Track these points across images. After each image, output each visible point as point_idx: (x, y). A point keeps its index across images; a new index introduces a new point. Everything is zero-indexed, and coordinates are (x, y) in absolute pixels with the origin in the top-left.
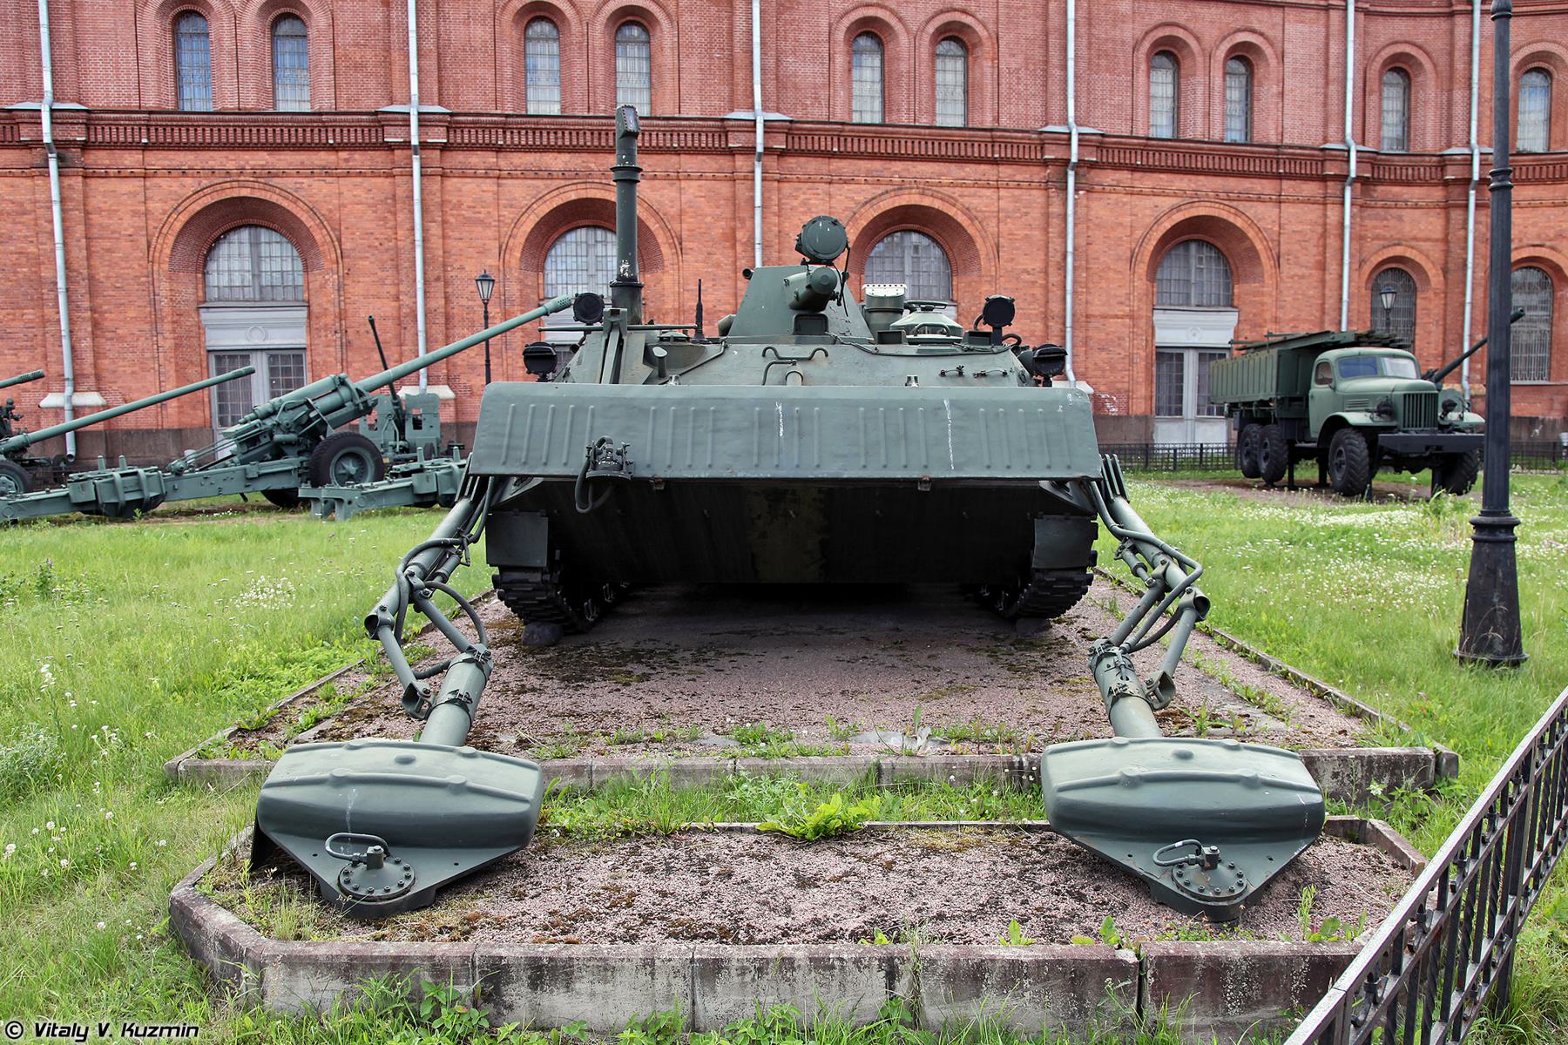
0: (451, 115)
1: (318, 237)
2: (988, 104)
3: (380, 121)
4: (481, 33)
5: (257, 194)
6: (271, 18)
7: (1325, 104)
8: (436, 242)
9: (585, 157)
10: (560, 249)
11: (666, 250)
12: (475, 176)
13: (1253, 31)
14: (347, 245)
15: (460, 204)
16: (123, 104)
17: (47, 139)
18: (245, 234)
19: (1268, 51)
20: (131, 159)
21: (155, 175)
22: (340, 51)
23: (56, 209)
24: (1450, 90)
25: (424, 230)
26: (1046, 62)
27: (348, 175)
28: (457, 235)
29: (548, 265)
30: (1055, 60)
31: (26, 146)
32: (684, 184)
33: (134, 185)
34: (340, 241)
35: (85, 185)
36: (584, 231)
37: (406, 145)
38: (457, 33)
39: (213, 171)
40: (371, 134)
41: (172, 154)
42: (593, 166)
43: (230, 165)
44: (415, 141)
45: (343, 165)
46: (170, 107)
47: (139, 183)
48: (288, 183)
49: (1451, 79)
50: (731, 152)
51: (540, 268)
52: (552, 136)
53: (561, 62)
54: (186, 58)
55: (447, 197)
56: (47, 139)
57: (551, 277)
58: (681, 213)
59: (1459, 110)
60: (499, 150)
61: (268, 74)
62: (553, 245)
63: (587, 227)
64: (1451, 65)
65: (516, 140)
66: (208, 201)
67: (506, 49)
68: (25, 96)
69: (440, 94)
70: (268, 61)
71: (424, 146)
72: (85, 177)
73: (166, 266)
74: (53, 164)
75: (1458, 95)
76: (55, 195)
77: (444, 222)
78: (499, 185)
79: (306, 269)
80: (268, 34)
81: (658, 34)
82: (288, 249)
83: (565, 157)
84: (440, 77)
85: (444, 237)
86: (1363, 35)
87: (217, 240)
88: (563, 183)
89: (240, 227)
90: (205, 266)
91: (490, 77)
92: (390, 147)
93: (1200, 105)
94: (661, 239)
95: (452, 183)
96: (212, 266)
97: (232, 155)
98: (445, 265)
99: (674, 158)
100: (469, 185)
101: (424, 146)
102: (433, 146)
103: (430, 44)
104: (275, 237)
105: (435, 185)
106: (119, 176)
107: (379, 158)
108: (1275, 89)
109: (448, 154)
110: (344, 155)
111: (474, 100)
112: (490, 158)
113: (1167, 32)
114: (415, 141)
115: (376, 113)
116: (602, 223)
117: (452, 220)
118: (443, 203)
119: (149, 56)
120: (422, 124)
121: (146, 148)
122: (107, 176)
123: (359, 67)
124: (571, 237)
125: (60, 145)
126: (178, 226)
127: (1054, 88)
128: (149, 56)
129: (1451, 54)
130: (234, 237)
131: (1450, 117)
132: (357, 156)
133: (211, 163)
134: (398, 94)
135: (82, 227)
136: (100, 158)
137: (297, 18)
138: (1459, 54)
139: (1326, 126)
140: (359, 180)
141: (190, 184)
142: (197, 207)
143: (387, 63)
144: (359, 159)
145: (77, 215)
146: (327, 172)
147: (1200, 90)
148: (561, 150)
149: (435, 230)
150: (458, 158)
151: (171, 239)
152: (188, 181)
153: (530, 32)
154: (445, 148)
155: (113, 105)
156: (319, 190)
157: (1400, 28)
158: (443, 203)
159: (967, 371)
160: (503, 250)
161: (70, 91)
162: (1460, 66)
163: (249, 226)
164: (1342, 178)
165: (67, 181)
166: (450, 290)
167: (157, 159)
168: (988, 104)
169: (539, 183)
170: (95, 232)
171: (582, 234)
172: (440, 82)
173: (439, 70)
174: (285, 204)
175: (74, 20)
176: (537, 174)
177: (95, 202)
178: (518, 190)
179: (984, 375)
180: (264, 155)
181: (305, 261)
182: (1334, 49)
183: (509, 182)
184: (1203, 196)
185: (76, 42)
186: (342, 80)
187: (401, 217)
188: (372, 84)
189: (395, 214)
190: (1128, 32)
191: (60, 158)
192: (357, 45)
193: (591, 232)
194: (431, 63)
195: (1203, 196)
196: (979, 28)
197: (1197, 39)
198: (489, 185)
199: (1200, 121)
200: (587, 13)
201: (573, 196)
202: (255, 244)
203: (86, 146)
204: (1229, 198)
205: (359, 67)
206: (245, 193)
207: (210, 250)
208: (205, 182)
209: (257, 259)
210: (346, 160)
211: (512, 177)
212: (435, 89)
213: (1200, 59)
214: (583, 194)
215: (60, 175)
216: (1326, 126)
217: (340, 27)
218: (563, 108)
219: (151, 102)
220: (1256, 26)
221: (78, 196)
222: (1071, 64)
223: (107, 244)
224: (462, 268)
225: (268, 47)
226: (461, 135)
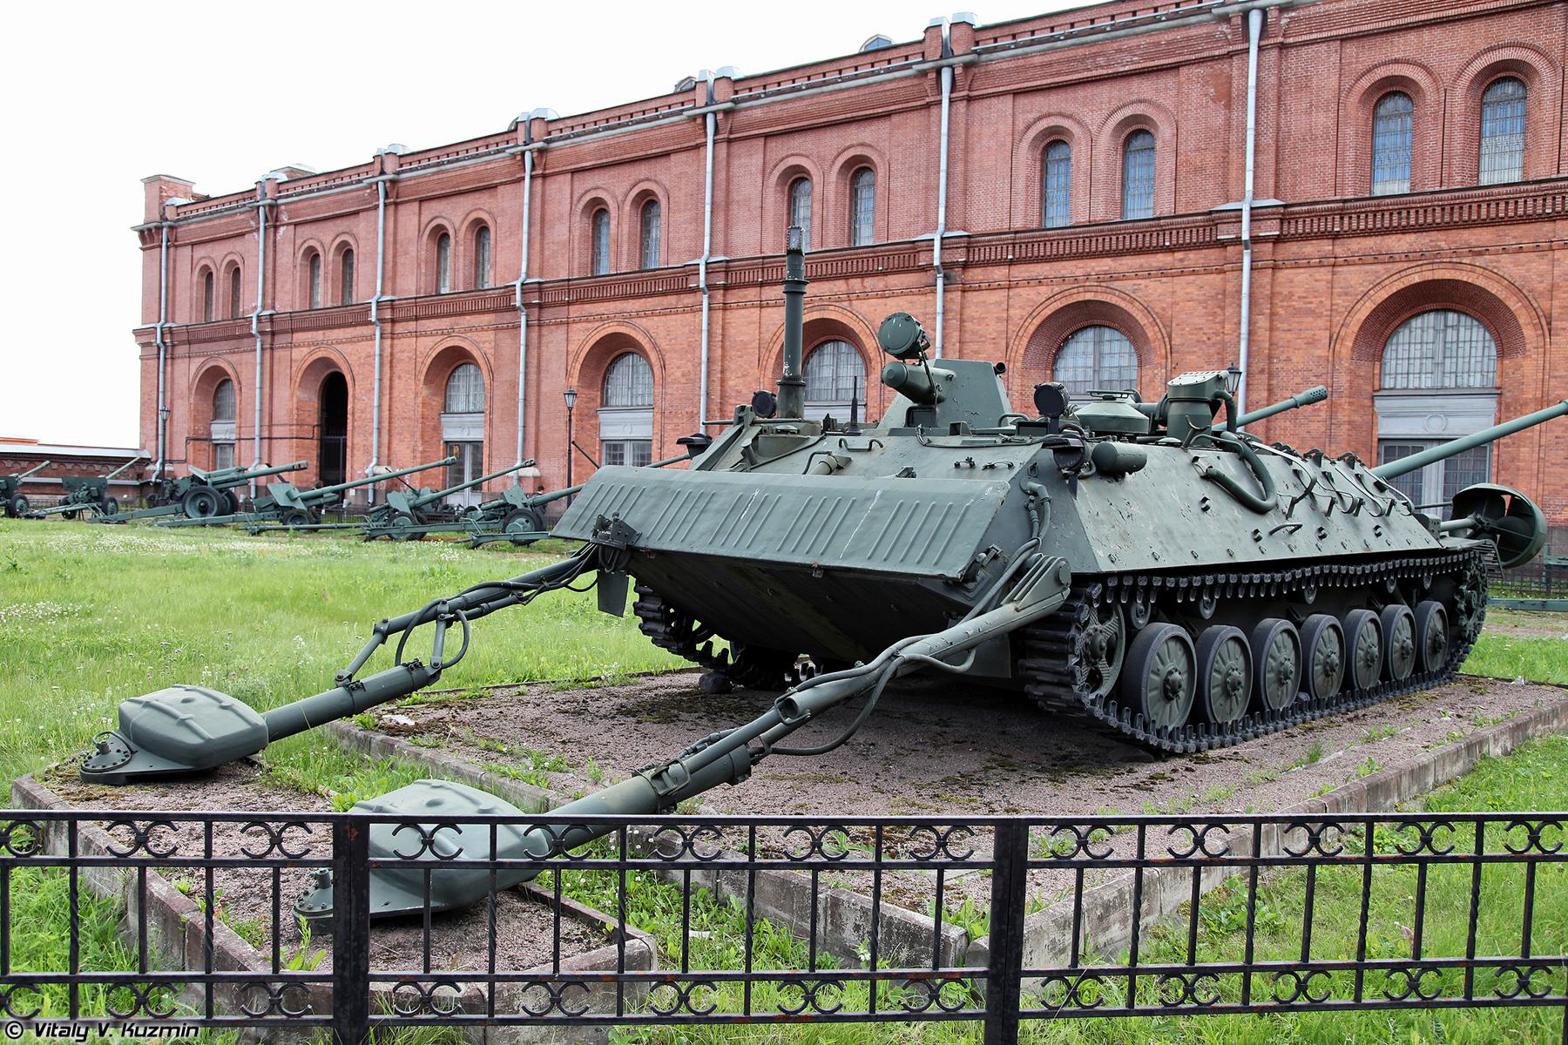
0: (1285, 206)
1: (1150, 334)
3: (1213, 219)
4: (1323, 120)
5: (1100, 298)
6: (1123, 136)
8: (1263, 335)
9: (1434, 235)
10: (1403, 335)
11: (1529, 332)
12: (1309, 266)
14: (1176, 341)
15: (1291, 294)
16: (997, 227)
17: (936, 263)
18: (1090, 334)
20: (999, 273)
21: (1017, 286)
22: (1182, 158)
23: (939, 319)
25: (1251, 322)
28: (1285, 326)
29: (1389, 353)
31: (923, 269)
32: (1558, 254)
33: (1000, 295)
34: (1170, 337)
35: (963, 297)
36: (1432, 316)
37: (1237, 241)
38: (1297, 123)
39: (1063, 278)
40: (1204, 234)
41: (1032, 267)
42: (1443, 244)
43: (1079, 272)
44: (1245, 236)
45: (1178, 265)
46: (1035, 226)
47: (1004, 293)
48: (1127, 285)
50: (1223, 244)
51: (1379, 357)
52: (1395, 217)
53: (1414, 136)
54: (1052, 182)
55: (1278, 289)
56: (936, 263)
57: (1390, 366)
58: (1553, 287)
60: (1335, 237)
61: (1118, 187)
62: (1395, 331)
63: (1437, 311)
65: (1354, 225)
66: (1058, 305)
67: (1349, 132)
68: (926, 230)
69: (1277, 186)
70: (1118, 175)
72: (964, 291)
73: (1019, 365)
74: (940, 282)
76: (939, 309)
77: (1272, 314)
78: (1334, 273)
79: (1140, 365)
80: (1120, 151)
81: (1537, 85)
82: (1126, 346)
83: (1411, 238)
84: (1277, 170)
85: (1271, 329)
87: (1066, 340)
88: (1406, 265)
89: (1086, 328)
90: (1055, 361)
91: (1330, 163)
92: (1223, 244)
94: (1523, 319)
95: (1283, 275)
96: (1061, 364)
97: (1080, 263)
98: (1270, 357)
99: (1548, 226)
100: (1301, 276)
101: (1255, 240)
102: (1265, 239)
103: (1268, 140)
104: (1117, 335)
105: (1265, 278)
106: (989, 289)
107: (1212, 255)
109: (1281, 246)
110: (1179, 255)
111: (1312, 187)
112: (1326, 246)
114: (1245, 236)
115: (1210, 213)
116: (1454, 306)
117: (1281, 311)
118: (1272, 295)
119: (1020, 184)
121: (1011, 263)
122: (980, 289)
123: (1198, 170)
124: (1416, 323)
125: (945, 265)
126: (1032, 329)
128: (1020, 184)
130: (1082, 337)
132: (1192, 255)
133: (1063, 272)
134: (1233, 192)
135: (957, 333)
136: (976, 274)
137: (1147, 132)
142: (1048, 312)
143: (1225, 163)
144: (1194, 258)
145: (955, 323)
146: (1163, 273)
148: (1405, 230)
149: (1262, 322)
150: (1292, 249)
151: (1025, 340)
152: (1043, 289)
153: (1382, 111)
154: (1277, 240)
155: (990, 229)
156: (1154, 290)
158: (1272, 295)
159: (980, 464)
160: (1333, 340)
161: (958, 222)
163: (1094, 326)
164: (696, 290)
165: (949, 296)
166: (1274, 382)
167: (1020, 272)
169: (1379, 267)
170: (967, 337)
171: (1430, 319)
172: (1277, 175)
173: (1277, 163)
174: (1123, 304)
175: (966, 162)
176: (1376, 259)
177: (969, 312)
178: (1355, 277)
179: (992, 467)
180: (1108, 261)
181: (1140, 357)
183: (1345, 269)
184: (1079, 279)
185: (966, 180)
186: (1181, 185)
187: (1229, 311)
188: (1210, 185)
189: (1223, 308)
191: (946, 277)
192: (1198, 150)
193: (1441, 317)
194: (1269, 158)
195: (1079, 279)
198: (1323, 274)
200: (1447, 79)
201: (1417, 279)
202: (1098, 342)
203: (966, 266)
204: (835, 299)
205: (1198, 170)
206: (1089, 296)
207: (1060, 349)
208: (1057, 289)
209: (1098, 356)
210: (1181, 260)
211: (1347, 263)
212: (1272, 182)
214: (1429, 276)
215: (945, 291)
217: (1182, 136)
218: (1413, 185)
219: (1018, 224)
221: (956, 307)
223: (975, 347)
224: (1288, 360)
225: (1119, 163)
226: (1292, 225)
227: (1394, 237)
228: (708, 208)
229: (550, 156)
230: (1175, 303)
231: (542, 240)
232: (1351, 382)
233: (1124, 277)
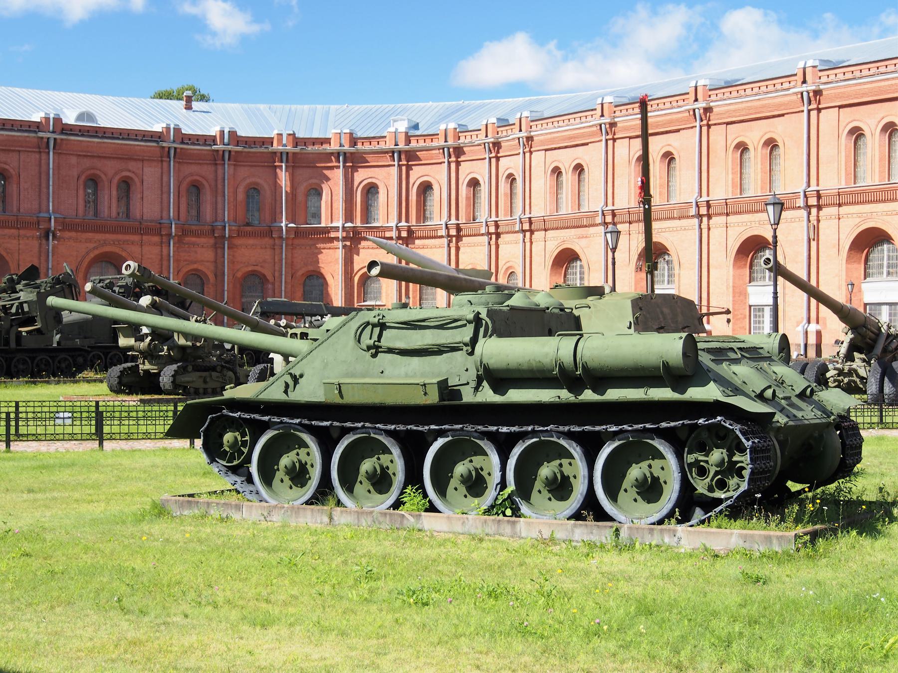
2: (15, 203)
7: (161, 203)
13: (130, 171)
19: (136, 179)
24: (216, 197)
26: (40, 185)
30: (44, 185)
49: (216, 191)
59: (220, 206)
64: (216, 186)
75: (219, 199)
86: (178, 172)
93: (106, 203)
108: (139, 196)
113: (92, 171)
127: (44, 197)
129: (216, 181)
131: (216, 209)
138: (219, 182)
139: (162, 212)
147: (106, 197)
157: (194, 169)
162: (220, 186)
168: (15, 203)
182: (165, 179)
190: (75, 173)
196: (11, 170)
197: (105, 175)
199: (106, 211)
213: (106, 183)
216: (162, 212)
220: (131, 168)
222: (51, 188)
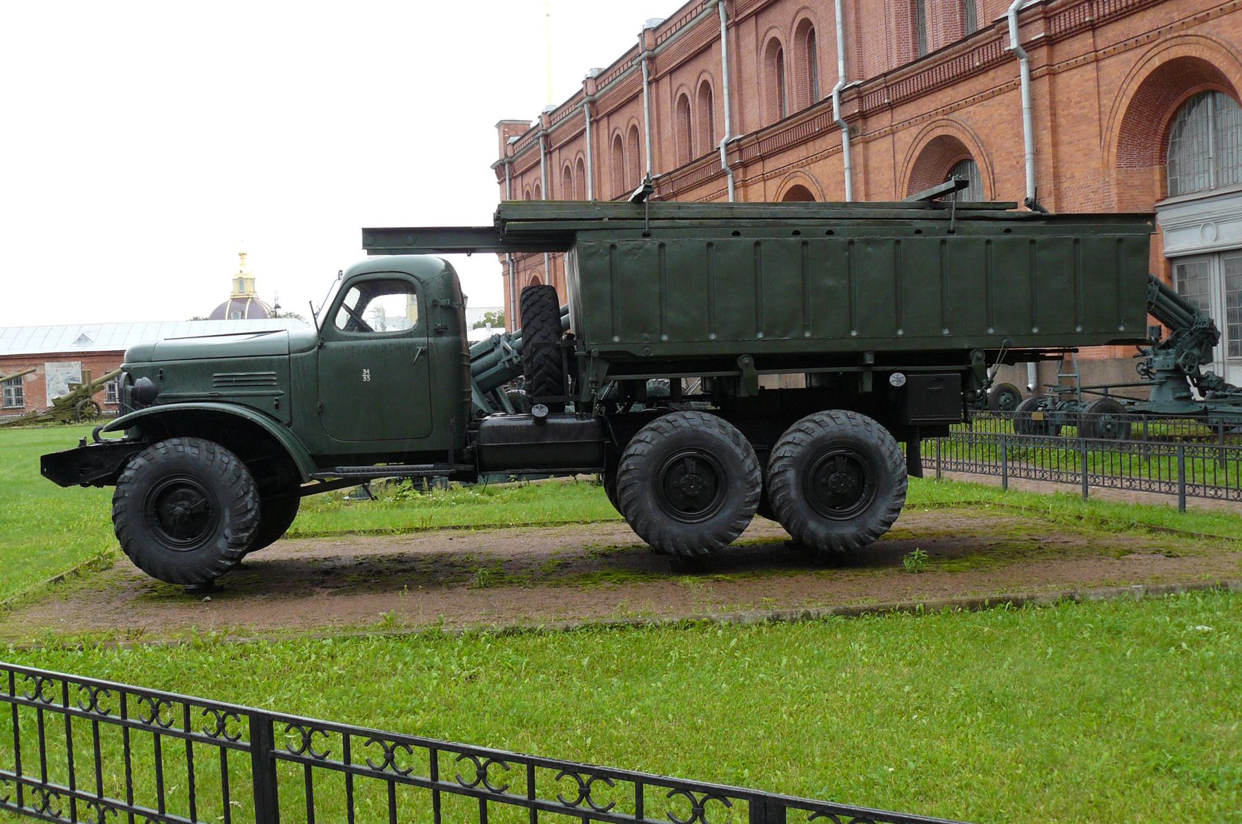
23: (847, 174)
27: (993, 95)
35: (866, 149)
47: (889, 138)
60: (1093, 27)
66: (922, 145)
71: (1029, 47)
105: (1044, 86)
110: (991, 74)
120: (1022, 25)
121: (891, 106)
140: (1002, 97)
141: (914, 130)
142: (917, 154)
145: (861, 176)
150: (1068, 49)
151: (906, 185)
154: (1051, 41)
177: (873, 163)
183: (1107, 62)
201: (1157, 62)
206: (939, 132)
221: (860, 160)
227: (1138, 16)
228: (726, 91)
229: (658, 61)
230: (994, 127)
231: (659, 138)
232: (1119, 194)
233: (959, 108)
